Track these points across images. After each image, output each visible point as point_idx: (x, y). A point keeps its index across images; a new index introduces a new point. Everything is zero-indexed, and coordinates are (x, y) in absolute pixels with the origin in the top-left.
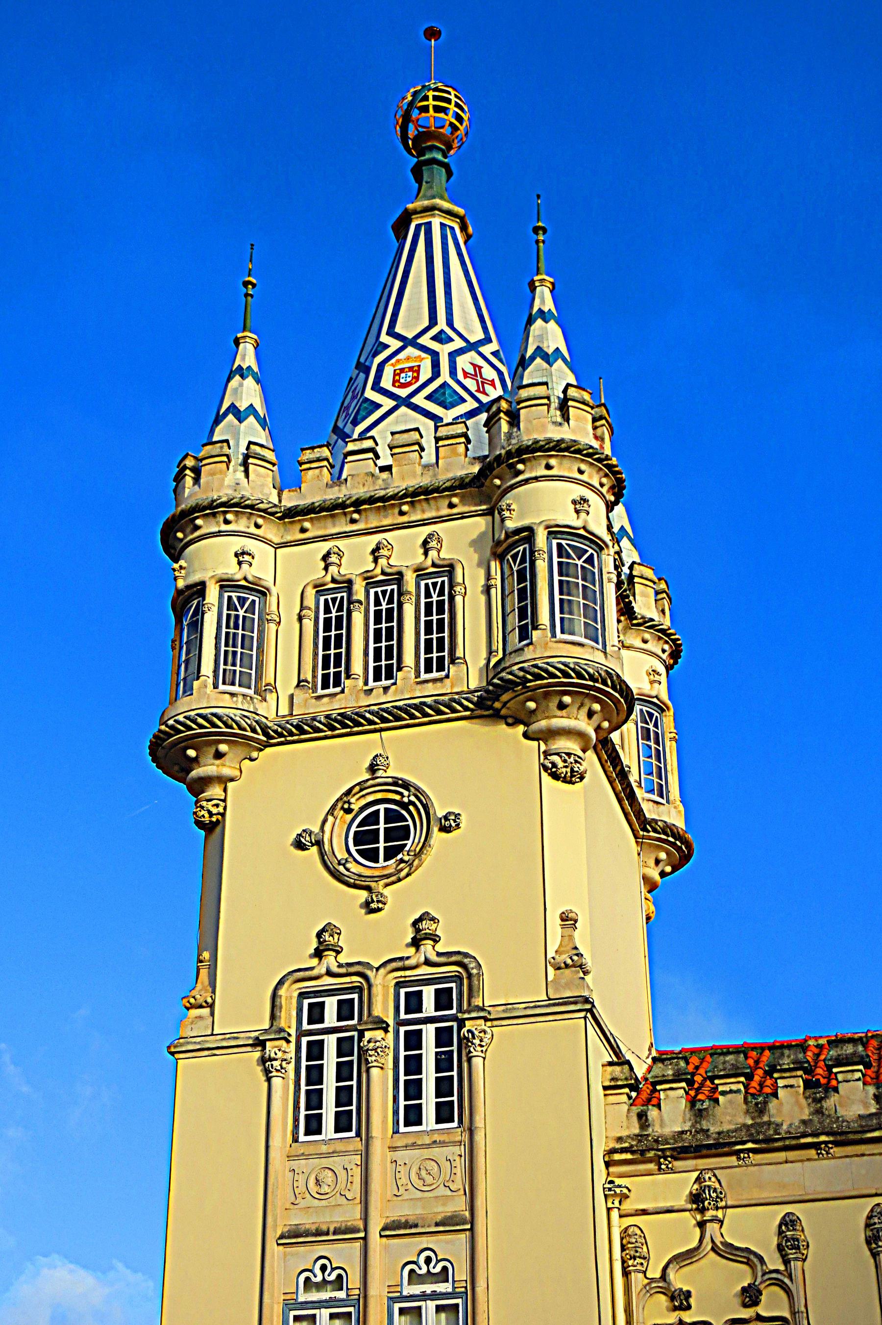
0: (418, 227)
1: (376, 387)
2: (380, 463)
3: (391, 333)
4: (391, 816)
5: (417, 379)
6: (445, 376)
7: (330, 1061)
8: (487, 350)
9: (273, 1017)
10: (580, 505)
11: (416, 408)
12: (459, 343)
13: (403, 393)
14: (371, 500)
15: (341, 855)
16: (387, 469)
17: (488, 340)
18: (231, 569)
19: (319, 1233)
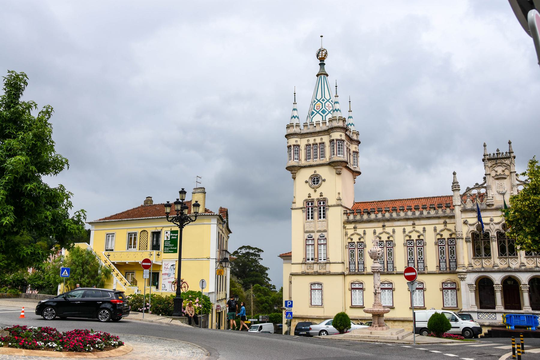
0: (320, 77)
1: (314, 109)
2: (314, 125)
3: (316, 99)
4: (317, 178)
5: (320, 108)
6: (324, 108)
7: (310, 210)
8: (330, 101)
9: (303, 205)
10: (341, 135)
11: (319, 114)
12: (326, 101)
13: (318, 110)
14: (313, 132)
15: (311, 184)
16: (315, 127)
17: (330, 98)
18: (295, 143)
19: (309, 231)
